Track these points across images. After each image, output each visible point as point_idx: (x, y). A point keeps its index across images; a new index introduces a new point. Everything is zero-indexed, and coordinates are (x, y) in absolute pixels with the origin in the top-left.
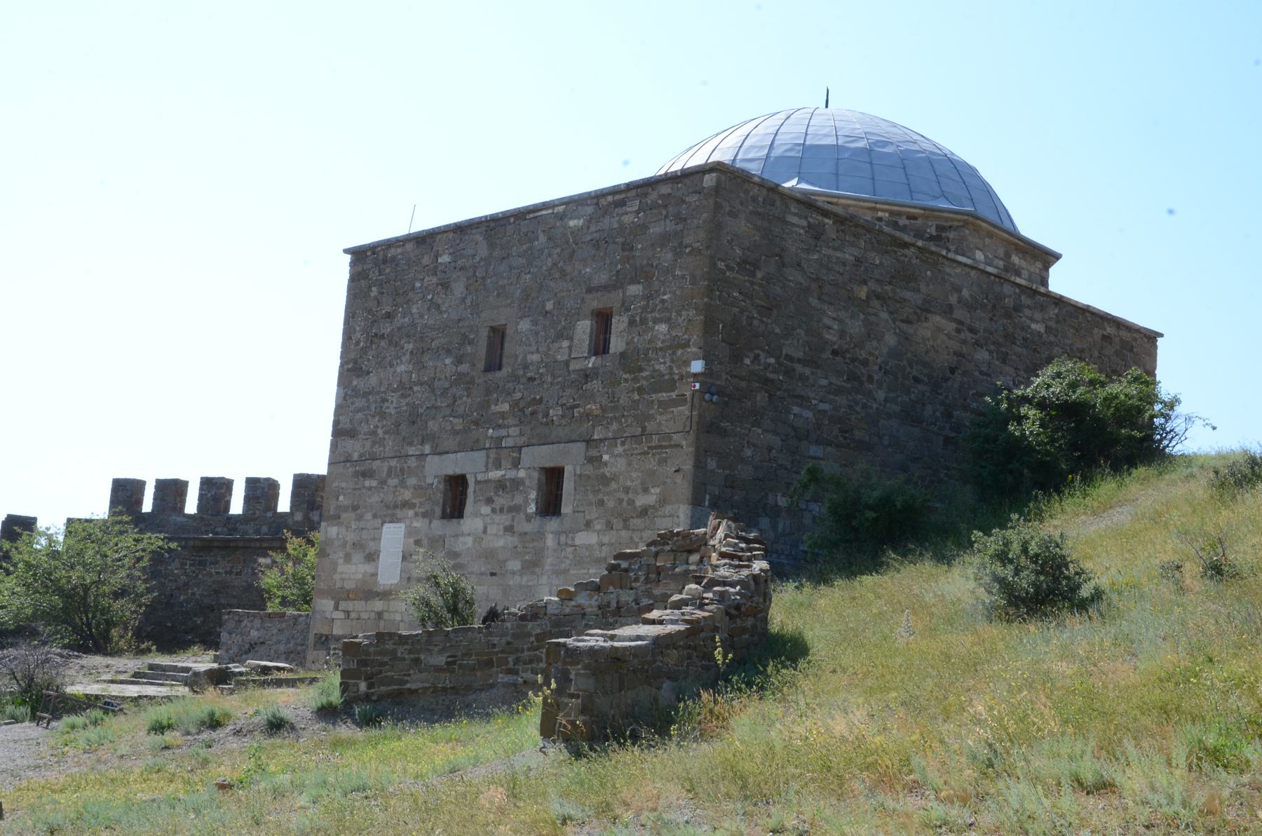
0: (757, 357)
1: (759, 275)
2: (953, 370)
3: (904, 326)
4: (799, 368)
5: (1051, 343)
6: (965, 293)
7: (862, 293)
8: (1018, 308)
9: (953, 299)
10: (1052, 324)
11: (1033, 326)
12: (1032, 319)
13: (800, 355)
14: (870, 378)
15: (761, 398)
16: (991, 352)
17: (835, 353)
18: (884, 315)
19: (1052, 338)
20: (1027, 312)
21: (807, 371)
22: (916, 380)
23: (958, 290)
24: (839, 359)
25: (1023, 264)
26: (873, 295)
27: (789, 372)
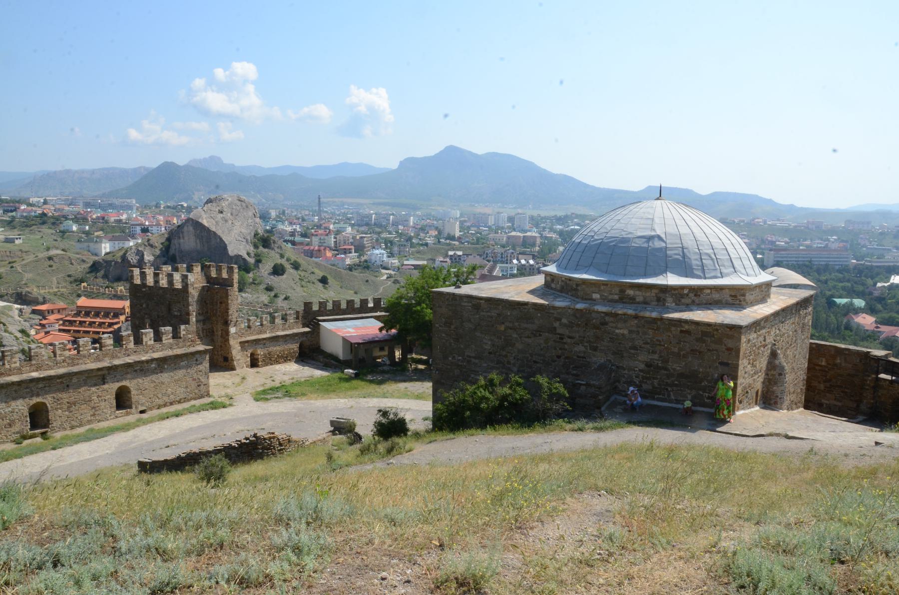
0: (454, 357)
1: (452, 327)
2: (559, 357)
3: (527, 340)
4: (473, 360)
5: (633, 339)
6: (564, 321)
7: (502, 328)
8: (604, 324)
9: (557, 324)
10: (634, 329)
11: (617, 331)
12: (616, 328)
13: (473, 355)
14: (509, 363)
15: (457, 372)
16: (585, 347)
17: (490, 353)
18: (515, 336)
19: (634, 336)
20: (611, 324)
21: (477, 361)
22: (535, 362)
23: (560, 320)
24: (492, 356)
25: (637, 293)
26: (507, 328)
27: (469, 362)
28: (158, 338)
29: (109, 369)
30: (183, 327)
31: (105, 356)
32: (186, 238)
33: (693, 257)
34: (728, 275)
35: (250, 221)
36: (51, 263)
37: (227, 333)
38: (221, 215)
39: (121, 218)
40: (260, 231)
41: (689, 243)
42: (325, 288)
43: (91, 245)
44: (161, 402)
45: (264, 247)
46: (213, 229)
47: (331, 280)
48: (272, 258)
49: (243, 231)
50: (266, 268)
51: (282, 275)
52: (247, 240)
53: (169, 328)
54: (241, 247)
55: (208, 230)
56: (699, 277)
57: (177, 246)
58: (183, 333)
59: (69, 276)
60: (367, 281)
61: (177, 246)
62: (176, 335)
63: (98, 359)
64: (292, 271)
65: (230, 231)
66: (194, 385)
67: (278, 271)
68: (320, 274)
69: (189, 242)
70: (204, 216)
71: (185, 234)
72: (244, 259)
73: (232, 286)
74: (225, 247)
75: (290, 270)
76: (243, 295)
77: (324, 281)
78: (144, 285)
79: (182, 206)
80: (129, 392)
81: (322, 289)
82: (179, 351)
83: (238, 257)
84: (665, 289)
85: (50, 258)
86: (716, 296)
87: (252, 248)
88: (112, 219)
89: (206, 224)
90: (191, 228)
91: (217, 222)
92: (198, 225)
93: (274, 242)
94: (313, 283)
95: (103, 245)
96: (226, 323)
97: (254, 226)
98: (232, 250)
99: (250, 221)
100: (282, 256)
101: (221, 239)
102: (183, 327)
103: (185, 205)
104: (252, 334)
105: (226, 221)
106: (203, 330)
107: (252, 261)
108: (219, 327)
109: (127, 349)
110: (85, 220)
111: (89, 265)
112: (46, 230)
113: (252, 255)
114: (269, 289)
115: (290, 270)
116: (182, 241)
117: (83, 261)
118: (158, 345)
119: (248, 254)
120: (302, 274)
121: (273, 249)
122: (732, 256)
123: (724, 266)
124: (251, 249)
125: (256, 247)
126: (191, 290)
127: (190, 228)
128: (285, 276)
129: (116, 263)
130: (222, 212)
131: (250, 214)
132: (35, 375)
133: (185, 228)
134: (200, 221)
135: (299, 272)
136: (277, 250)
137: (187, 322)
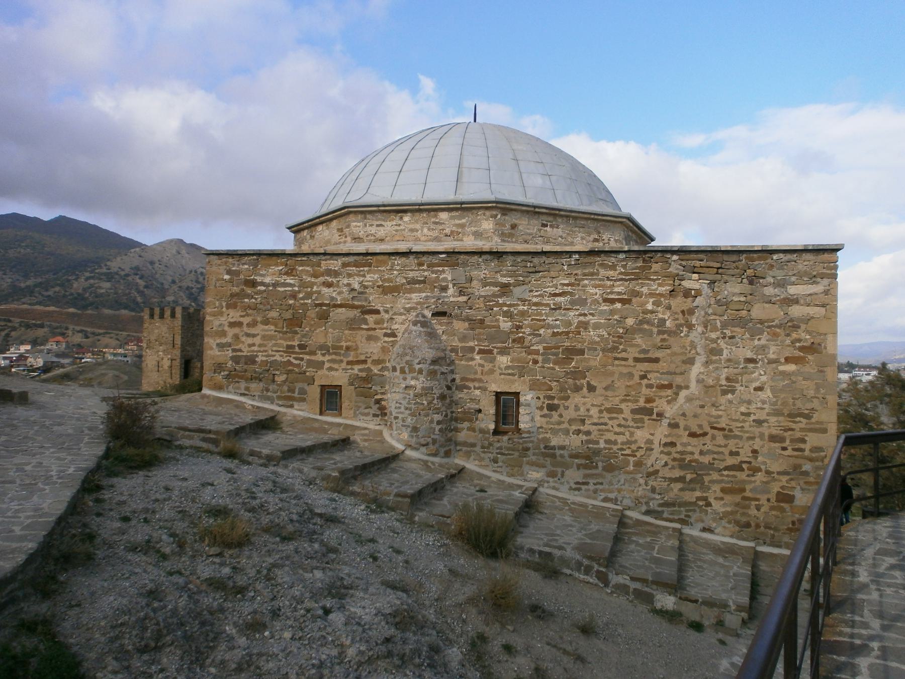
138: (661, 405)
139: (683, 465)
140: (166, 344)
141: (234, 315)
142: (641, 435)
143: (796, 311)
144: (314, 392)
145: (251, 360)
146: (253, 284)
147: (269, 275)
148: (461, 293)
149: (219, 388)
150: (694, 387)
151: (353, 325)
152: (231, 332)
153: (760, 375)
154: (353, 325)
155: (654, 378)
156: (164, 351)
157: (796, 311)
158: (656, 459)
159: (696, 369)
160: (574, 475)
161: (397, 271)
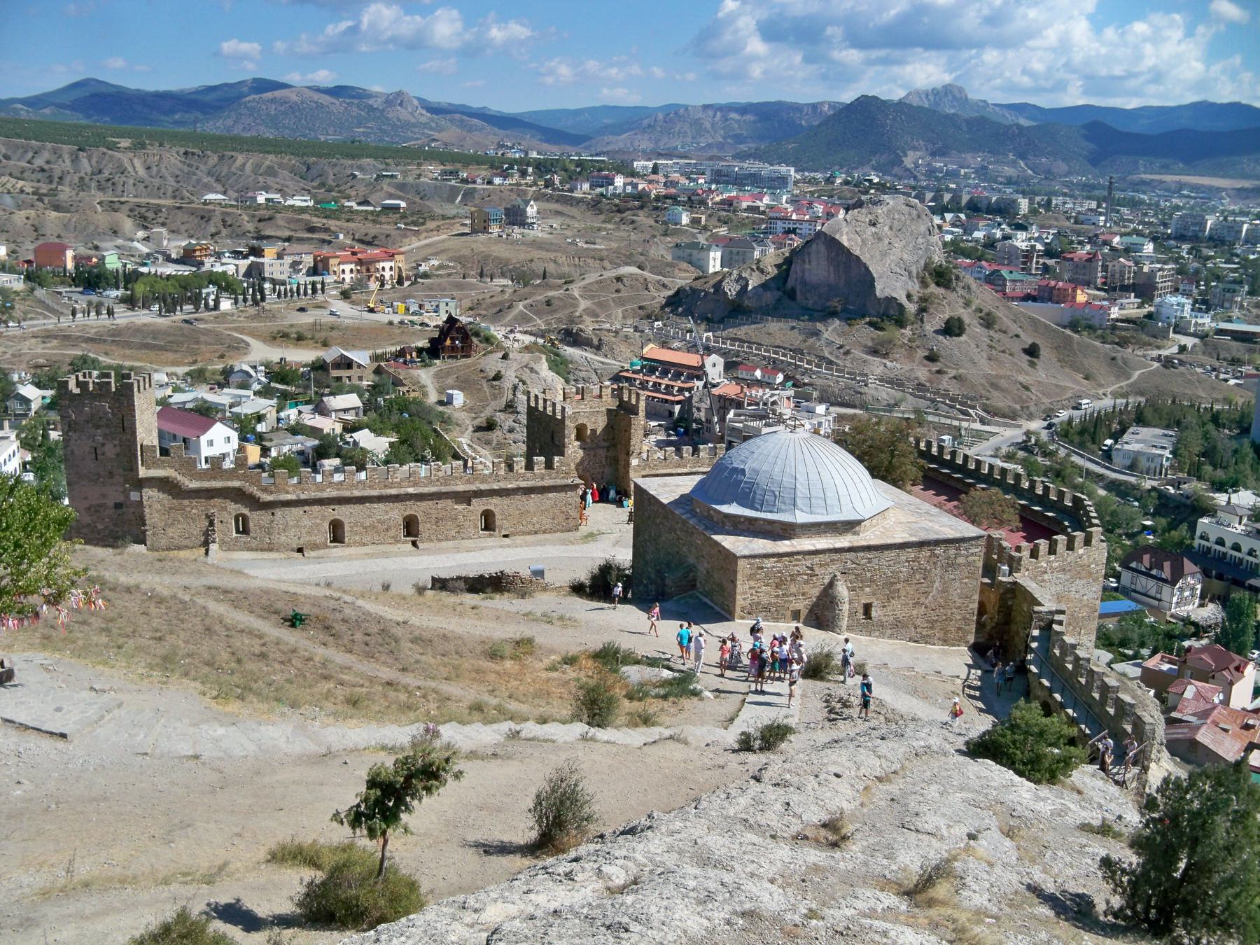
28: (529, 466)
29: (475, 492)
30: (556, 458)
31: (476, 479)
32: (814, 263)
33: (759, 492)
34: (783, 511)
35: (920, 240)
36: (620, 285)
37: (628, 464)
38: (874, 229)
39: (758, 203)
40: (936, 259)
41: (762, 480)
42: (1032, 365)
43: (695, 252)
44: (524, 529)
45: (938, 284)
46: (857, 252)
47: (1044, 352)
48: (949, 306)
49: (906, 257)
50: (934, 322)
51: (959, 335)
52: (910, 273)
53: (542, 459)
54: (898, 284)
55: (847, 252)
56: (757, 510)
57: (800, 274)
58: (556, 464)
59: (640, 308)
60: (1113, 359)
61: (800, 274)
62: (549, 465)
63: (468, 482)
64: (979, 330)
65: (884, 254)
66: (561, 517)
67: (952, 328)
68: (1028, 340)
69: (817, 269)
70: (845, 230)
71: (813, 256)
72: (901, 306)
73: (637, 414)
74: (868, 280)
75: (974, 327)
76: (889, 364)
77: (1032, 351)
78: (536, 408)
79: (870, 181)
80: (494, 515)
81: (1025, 366)
82: (548, 482)
83: (891, 300)
84: (727, 516)
85: (619, 279)
86: (768, 527)
87: (917, 287)
88: (745, 205)
89: (846, 244)
90: (822, 248)
91: (863, 241)
92: (833, 244)
93: (957, 278)
94: (1011, 355)
95: (712, 254)
96: (628, 454)
97: (927, 250)
98: (881, 290)
99: (920, 240)
100: (967, 304)
101: (867, 269)
102: (556, 458)
103: (876, 180)
104: (667, 467)
105: (880, 239)
106: (606, 457)
107: (911, 308)
108: (622, 457)
109: (497, 475)
110: (703, 203)
111: (670, 293)
112: (643, 219)
113: (915, 299)
114: (932, 358)
115: (974, 327)
116: (807, 266)
117: (664, 286)
118: (529, 474)
119: (909, 296)
120: (996, 336)
121: (954, 289)
122: (798, 494)
123: (784, 503)
124: (915, 287)
125: (924, 284)
126: (567, 422)
127: (820, 248)
128: (964, 338)
129: (707, 293)
130: (874, 225)
131: (923, 229)
132: (411, 490)
133: (814, 246)
134: (837, 237)
135: (992, 333)
136: (961, 292)
137: (562, 454)
138: (922, 600)
139: (928, 622)
140: (108, 426)
141: (752, 583)
142: (915, 612)
143: (971, 558)
144: (789, 614)
145: (758, 604)
146: (762, 568)
147: (769, 563)
148: (853, 563)
149: (743, 618)
150: (935, 592)
151: (806, 582)
152: (750, 592)
153: (957, 584)
154: (806, 582)
155: (923, 590)
156: (105, 436)
157: (971, 558)
158: (918, 622)
159: (937, 584)
160: (889, 632)
161: (826, 557)
